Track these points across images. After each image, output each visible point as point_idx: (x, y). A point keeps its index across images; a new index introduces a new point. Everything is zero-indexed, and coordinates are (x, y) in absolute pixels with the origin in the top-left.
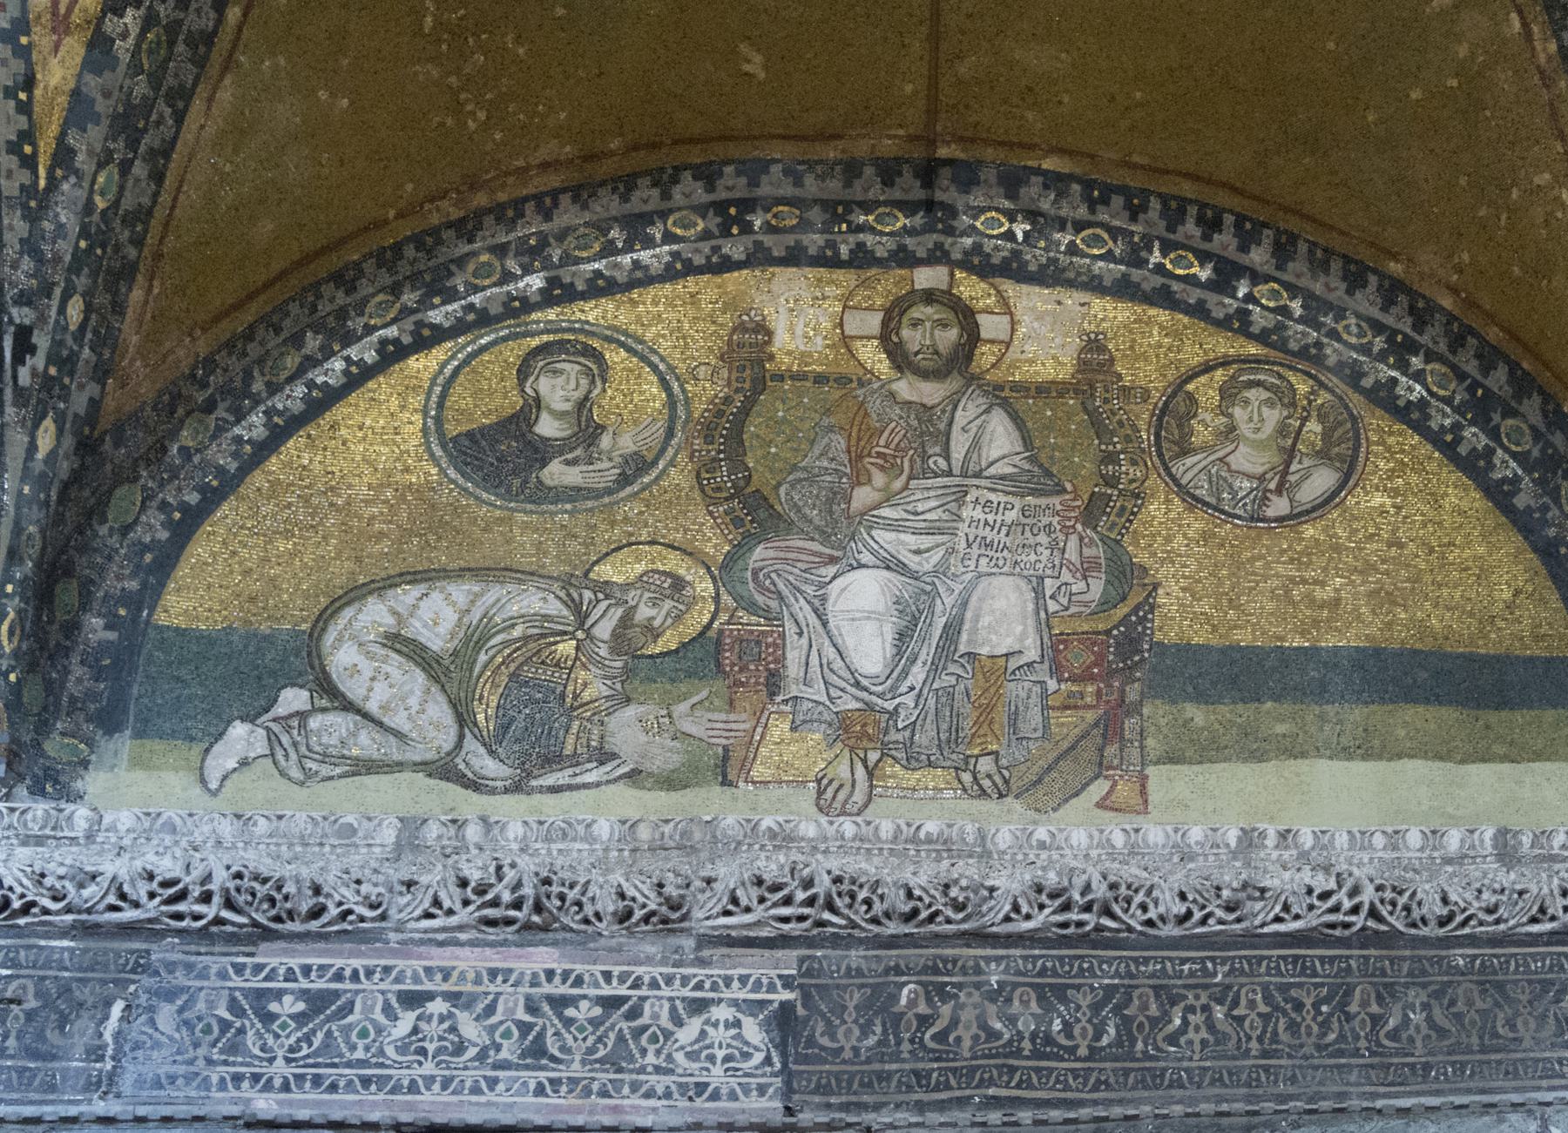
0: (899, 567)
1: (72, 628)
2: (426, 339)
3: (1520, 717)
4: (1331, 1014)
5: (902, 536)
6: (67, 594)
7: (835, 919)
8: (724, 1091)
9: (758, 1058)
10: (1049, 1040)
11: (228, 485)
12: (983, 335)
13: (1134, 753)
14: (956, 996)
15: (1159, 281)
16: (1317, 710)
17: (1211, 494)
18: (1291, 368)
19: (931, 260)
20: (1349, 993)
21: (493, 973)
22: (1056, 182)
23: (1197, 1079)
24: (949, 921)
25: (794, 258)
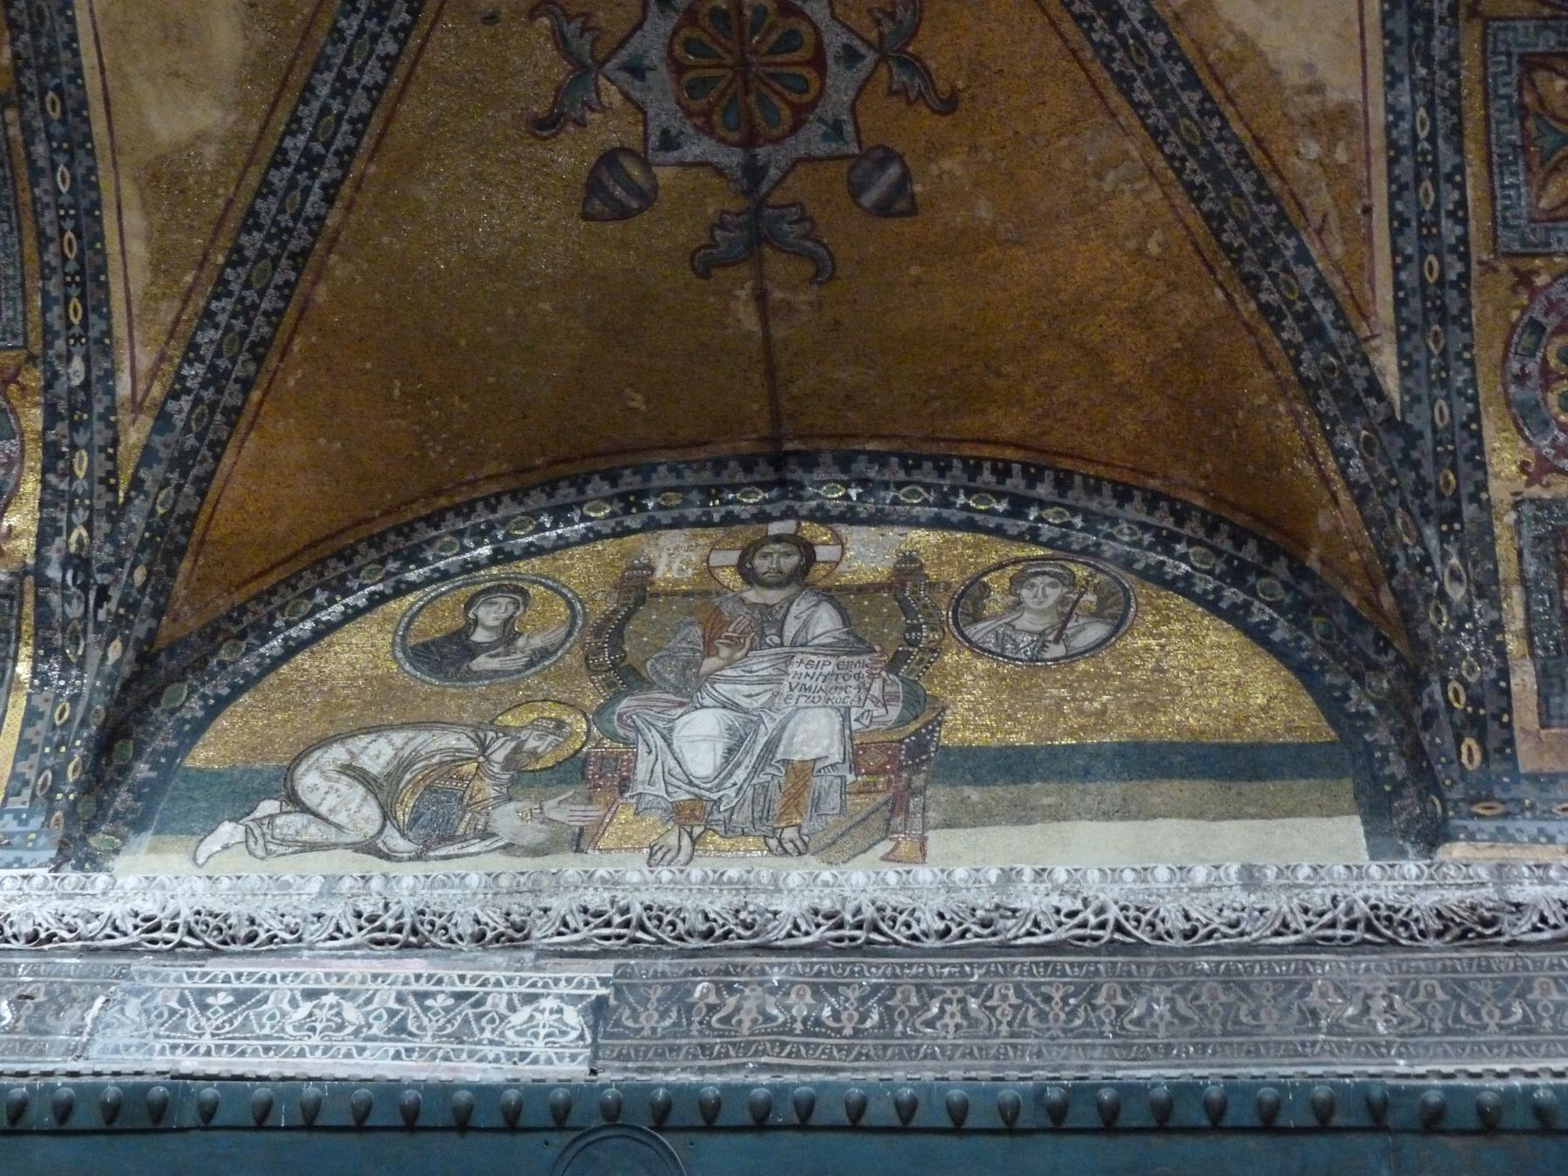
1: (125, 770)
2: (400, 591)
4: (1078, 1006)
5: (739, 687)
7: (646, 937)
8: (543, 1058)
9: (574, 1035)
10: (818, 1022)
11: (251, 682)
12: (819, 558)
13: (917, 822)
14: (742, 991)
15: (964, 515)
16: (1080, 786)
17: (996, 645)
18: (1072, 561)
19: (784, 516)
20: (1096, 989)
21: (375, 977)
22: (879, 458)
23: (949, 1053)
24: (740, 937)
25: (676, 524)
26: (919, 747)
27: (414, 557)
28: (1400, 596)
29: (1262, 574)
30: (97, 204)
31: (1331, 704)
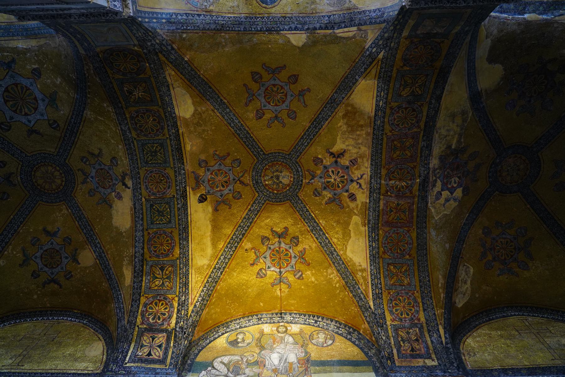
0: (280, 353)
1: (186, 362)
2: (226, 333)
3: (361, 367)
6: (186, 358)
11: (204, 347)
22: (295, 314)
25: (266, 323)
26: (308, 361)
27: (228, 327)
28: (375, 338)
29: (353, 334)
30: (189, 274)
31: (366, 354)
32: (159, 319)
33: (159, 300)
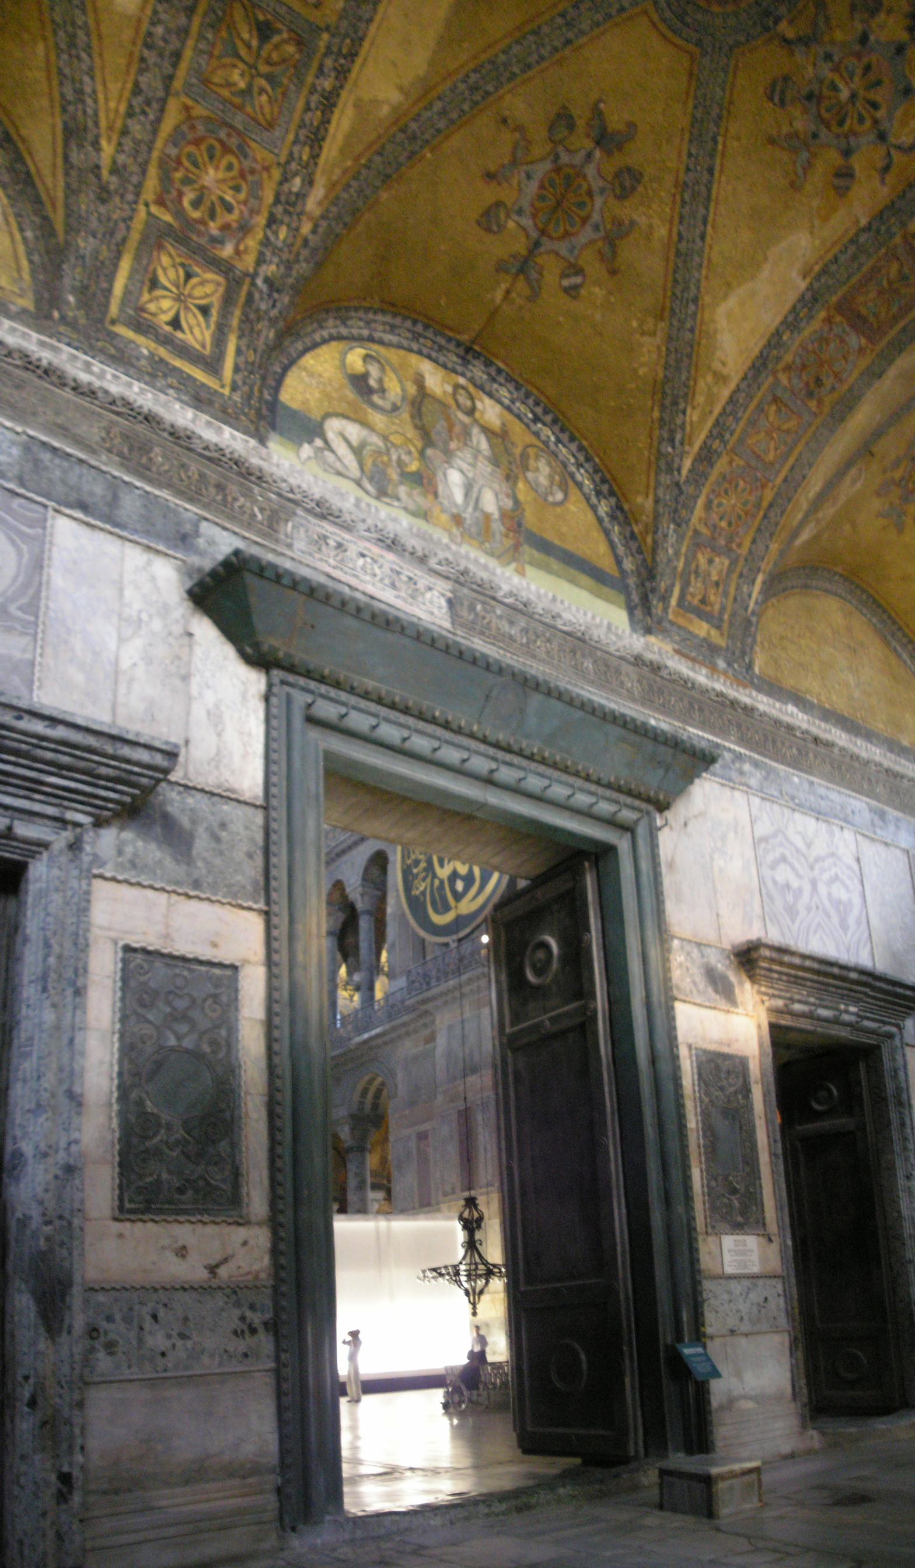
32: (212, 216)
33: (222, 143)
